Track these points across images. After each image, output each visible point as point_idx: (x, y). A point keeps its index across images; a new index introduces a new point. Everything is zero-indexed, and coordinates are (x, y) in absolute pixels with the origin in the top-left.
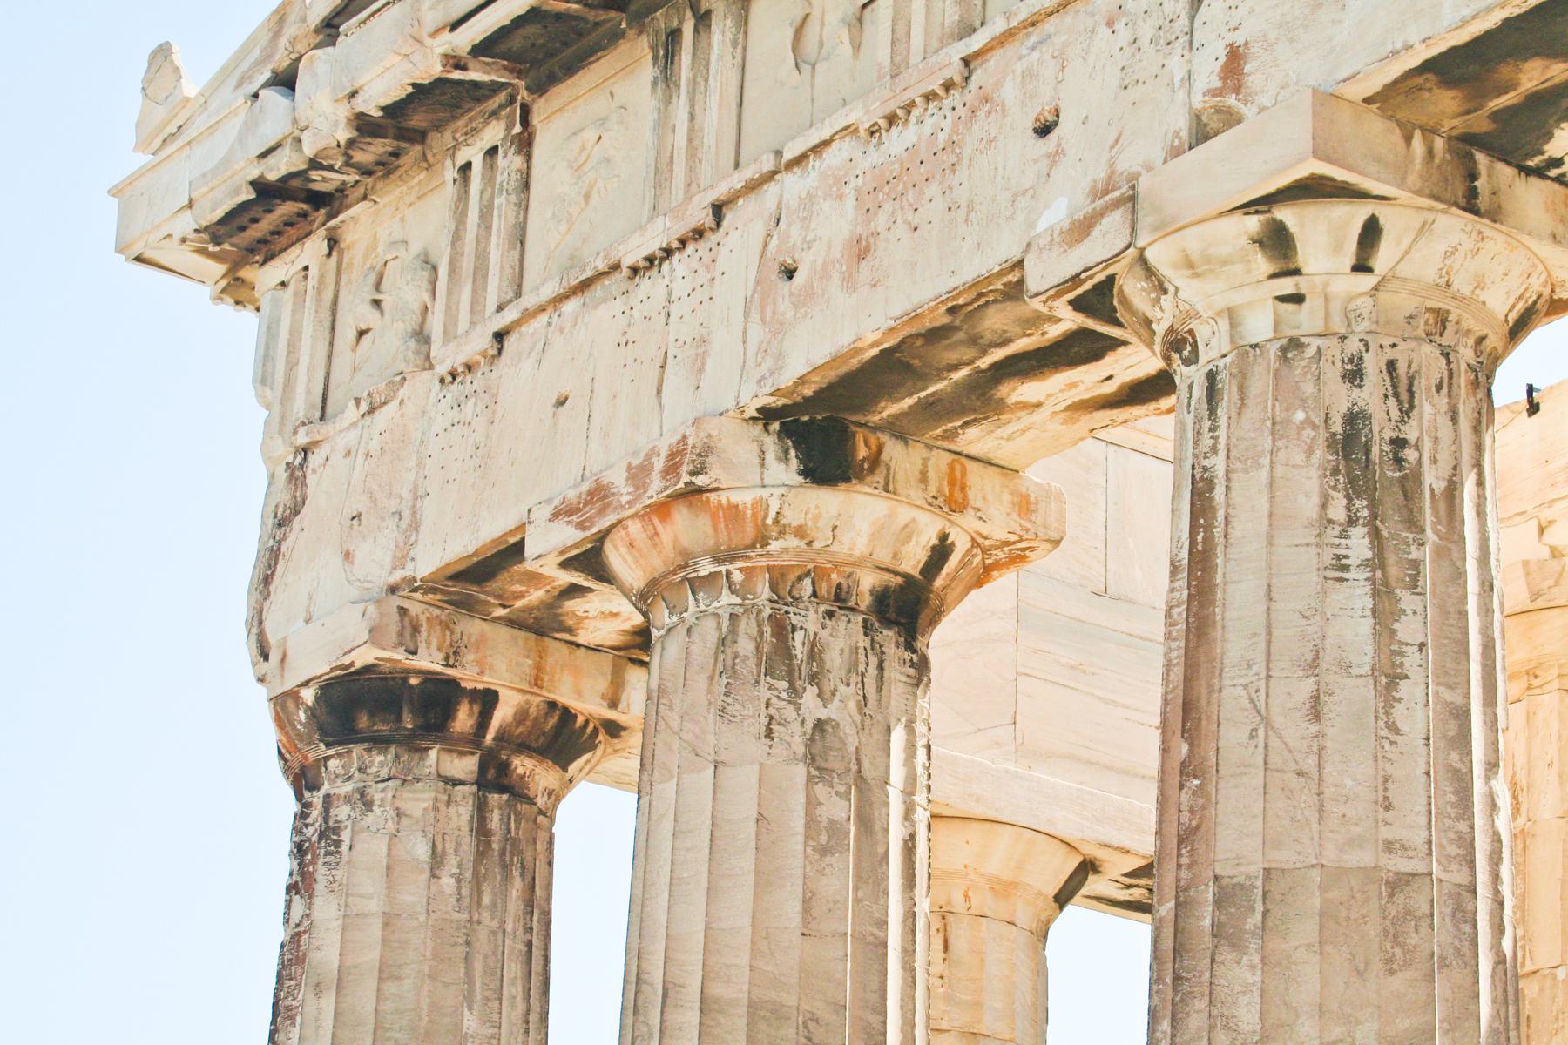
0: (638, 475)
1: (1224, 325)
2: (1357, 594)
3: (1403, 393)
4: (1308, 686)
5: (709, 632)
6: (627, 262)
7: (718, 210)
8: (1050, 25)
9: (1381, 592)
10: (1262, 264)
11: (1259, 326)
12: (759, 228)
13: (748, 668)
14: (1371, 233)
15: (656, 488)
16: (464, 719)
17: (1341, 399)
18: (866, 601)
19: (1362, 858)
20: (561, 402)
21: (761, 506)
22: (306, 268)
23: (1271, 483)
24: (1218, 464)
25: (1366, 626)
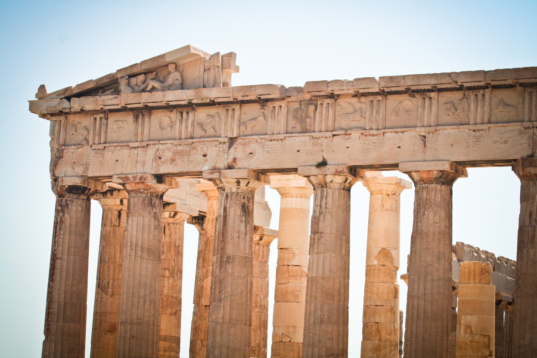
0: (135, 178)
1: (229, 189)
2: (243, 224)
3: (249, 200)
4: (238, 235)
5: (141, 200)
6: (131, 146)
7: (147, 145)
8: (206, 143)
9: (246, 224)
10: (236, 184)
11: (234, 190)
12: (155, 150)
13: (147, 204)
14: (249, 183)
15: (138, 180)
16: (87, 192)
17: (243, 201)
18: (159, 196)
19: (243, 255)
20: (117, 161)
21: (151, 185)
22: (61, 120)
23: (235, 210)
24: (228, 206)
25: (244, 228)
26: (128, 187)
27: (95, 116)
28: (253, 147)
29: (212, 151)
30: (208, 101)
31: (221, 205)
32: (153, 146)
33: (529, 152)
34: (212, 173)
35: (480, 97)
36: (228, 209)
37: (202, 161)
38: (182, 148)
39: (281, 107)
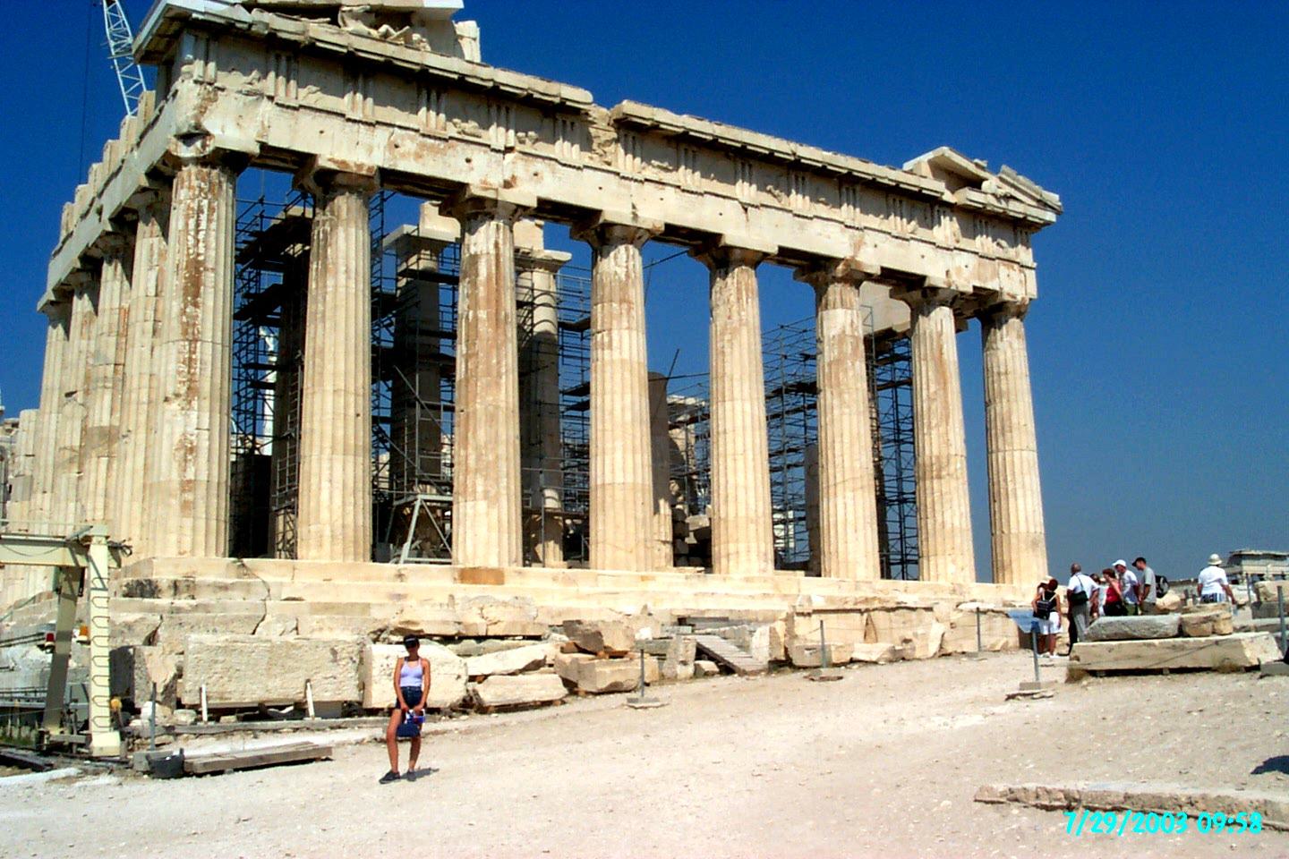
6: (347, 116)
15: (364, 172)
20: (322, 132)
24: (501, 242)
26: (340, 179)
27: (278, 52)
28: (539, 166)
29: (480, 157)
30: (490, 84)
31: (488, 239)
32: (385, 128)
33: (852, 254)
34: (486, 189)
35: (800, 179)
36: (501, 246)
37: (465, 169)
38: (432, 141)
39: (572, 124)
